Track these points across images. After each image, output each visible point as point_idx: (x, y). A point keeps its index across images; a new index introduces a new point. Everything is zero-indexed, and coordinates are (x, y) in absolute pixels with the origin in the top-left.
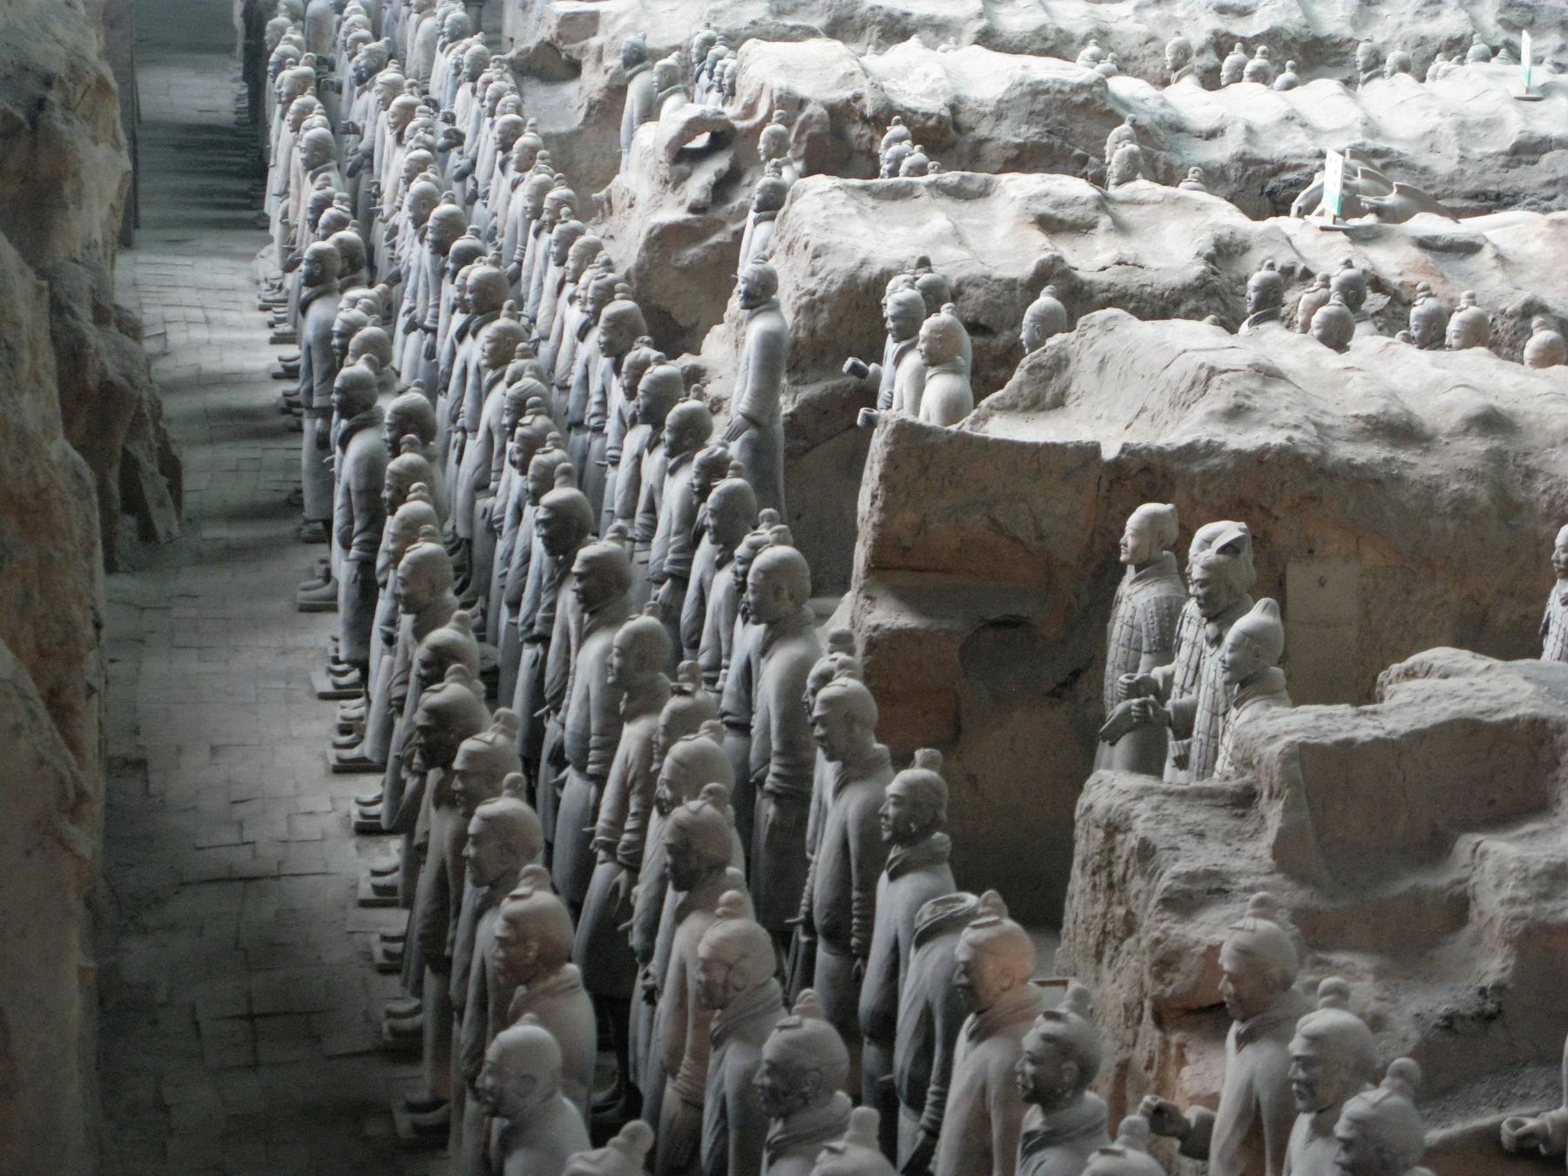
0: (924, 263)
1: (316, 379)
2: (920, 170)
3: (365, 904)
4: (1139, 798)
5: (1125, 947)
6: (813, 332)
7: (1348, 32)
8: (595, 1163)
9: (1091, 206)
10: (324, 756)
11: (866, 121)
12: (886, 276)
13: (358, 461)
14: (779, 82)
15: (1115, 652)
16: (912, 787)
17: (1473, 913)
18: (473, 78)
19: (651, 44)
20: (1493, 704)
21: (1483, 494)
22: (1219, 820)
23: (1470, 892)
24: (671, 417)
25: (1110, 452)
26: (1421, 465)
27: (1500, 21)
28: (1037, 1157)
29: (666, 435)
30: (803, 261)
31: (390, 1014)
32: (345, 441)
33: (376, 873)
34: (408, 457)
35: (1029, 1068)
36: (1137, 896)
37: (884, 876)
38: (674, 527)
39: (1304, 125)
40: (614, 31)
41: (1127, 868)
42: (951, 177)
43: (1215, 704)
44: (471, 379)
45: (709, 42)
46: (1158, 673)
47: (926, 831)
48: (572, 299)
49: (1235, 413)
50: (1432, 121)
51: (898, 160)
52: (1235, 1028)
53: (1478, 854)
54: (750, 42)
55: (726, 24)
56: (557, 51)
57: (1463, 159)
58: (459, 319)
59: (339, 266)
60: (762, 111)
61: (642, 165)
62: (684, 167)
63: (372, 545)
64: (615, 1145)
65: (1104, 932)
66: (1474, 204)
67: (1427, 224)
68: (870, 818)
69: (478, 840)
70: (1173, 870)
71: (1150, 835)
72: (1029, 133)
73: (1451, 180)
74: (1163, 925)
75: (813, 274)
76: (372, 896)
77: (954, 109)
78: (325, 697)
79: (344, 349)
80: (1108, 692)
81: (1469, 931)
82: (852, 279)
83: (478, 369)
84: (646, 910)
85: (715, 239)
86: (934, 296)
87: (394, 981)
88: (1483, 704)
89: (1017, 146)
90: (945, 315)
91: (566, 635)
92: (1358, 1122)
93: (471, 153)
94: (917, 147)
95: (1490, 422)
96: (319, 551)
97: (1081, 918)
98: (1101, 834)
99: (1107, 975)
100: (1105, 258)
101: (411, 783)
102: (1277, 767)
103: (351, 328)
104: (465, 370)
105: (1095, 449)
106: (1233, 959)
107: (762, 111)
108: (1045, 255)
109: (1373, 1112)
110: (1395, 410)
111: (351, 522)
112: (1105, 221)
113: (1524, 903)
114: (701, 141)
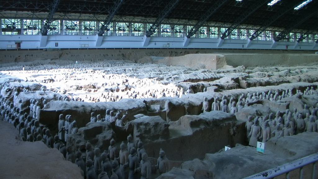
2: (28, 91)
14: (14, 85)
15: (59, 126)
17: (99, 140)
21: (83, 111)
22: (79, 136)
25: (56, 111)
26: (78, 110)
37: (54, 143)
45: (5, 83)
46: (64, 127)
49: (65, 107)
52: (87, 151)
55: (6, 81)
70: (76, 141)
72: (34, 88)
77: (28, 86)
82: (27, 100)
86: (35, 101)
92: (103, 155)
95: (83, 106)
98: (70, 139)
105: (55, 111)
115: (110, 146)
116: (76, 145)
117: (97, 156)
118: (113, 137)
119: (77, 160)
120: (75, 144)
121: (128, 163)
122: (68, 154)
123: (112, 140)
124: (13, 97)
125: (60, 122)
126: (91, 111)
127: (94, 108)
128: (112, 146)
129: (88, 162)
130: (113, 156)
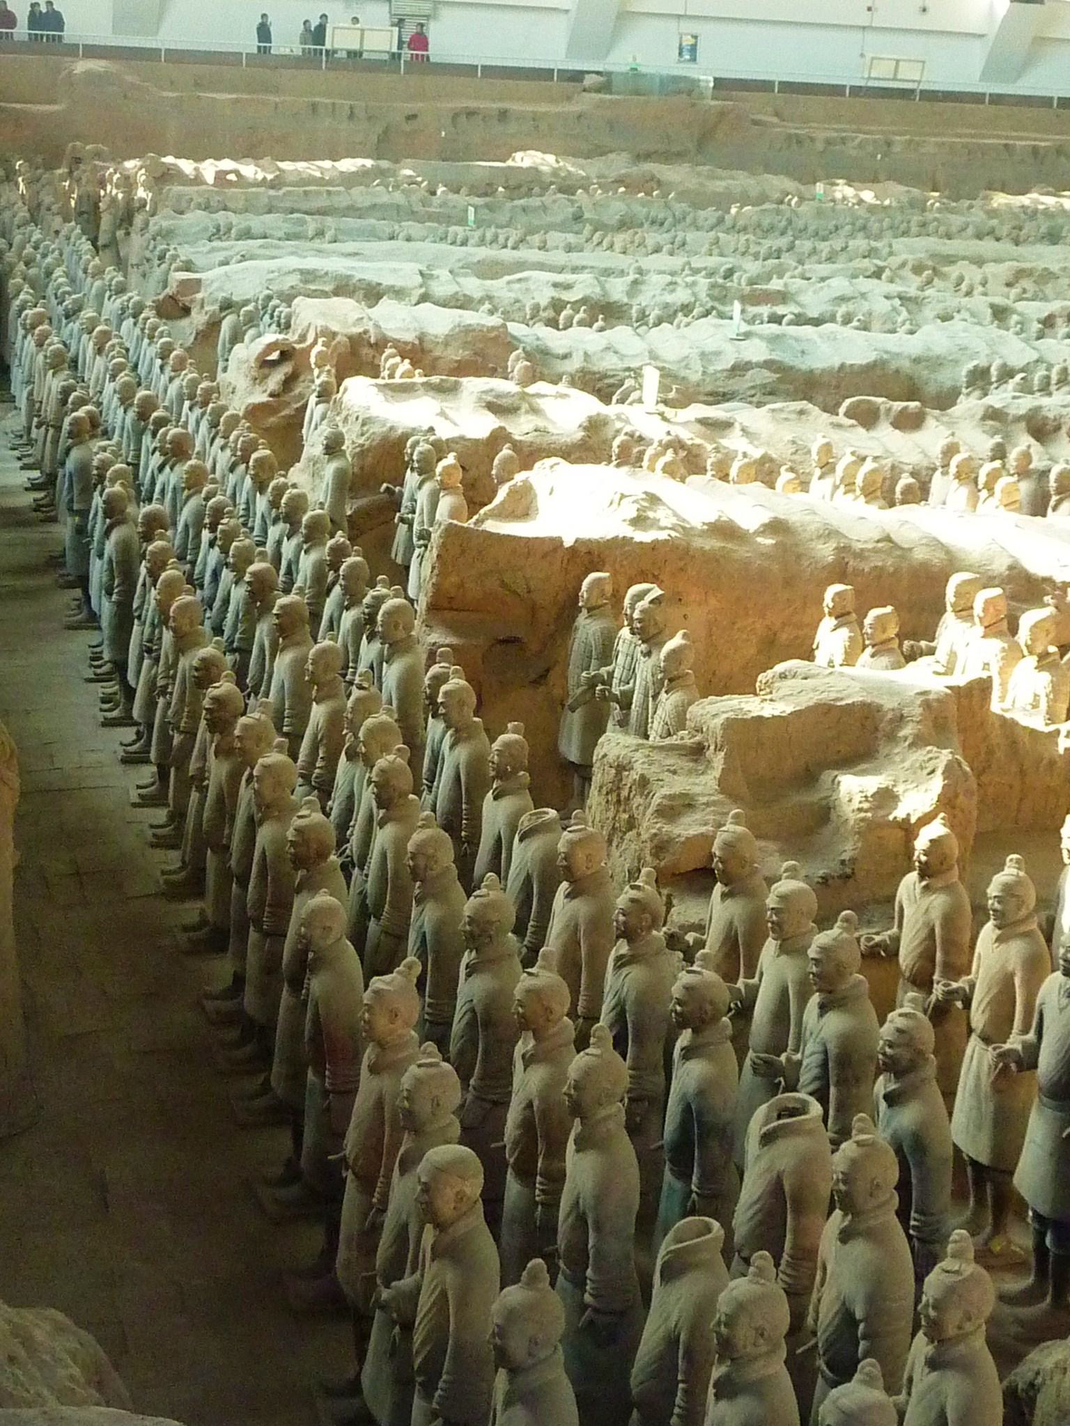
0: (431, 430)
1: (75, 492)
3: (135, 805)
4: (637, 750)
5: (627, 836)
6: (362, 468)
7: (626, 300)
8: (388, 984)
9: (517, 397)
10: (94, 717)
11: (371, 346)
12: (405, 437)
13: (117, 544)
14: (320, 323)
16: (507, 745)
17: (833, 816)
18: (135, 316)
19: (235, 298)
20: (839, 695)
22: (686, 764)
23: (831, 805)
24: (305, 519)
25: (568, 543)
26: (742, 552)
27: (708, 295)
28: (625, 971)
29: (303, 530)
30: (357, 428)
31: (163, 873)
32: (107, 533)
33: (139, 787)
34: (158, 543)
35: (621, 918)
36: (637, 808)
37: (490, 795)
38: (308, 584)
39: (616, 352)
40: (210, 290)
41: (630, 792)
42: (435, 379)
43: (646, 689)
44: (169, 496)
45: (269, 298)
47: (515, 771)
48: (223, 448)
50: (686, 352)
51: (395, 367)
52: (719, 888)
53: (835, 784)
54: (299, 298)
55: (275, 287)
56: (176, 301)
57: (704, 373)
58: (157, 459)
59: (88, 427)
60: (310, 340)
61: (239, 369)
62: (266, 371)
63: (128, 593)
64: (398, 972)
65: (613, 828)
66: (711, 399)
67: (699, 410)
68: (476, 764)
69: (260, 779)
71: (645, 772)
73: (698, 385)
74: (658, 825)
75: (362, 435)
76: (138, 800)
77: (421, 338)
78: (90, 681)
79: (101, 478)
80: (571, 682)
81: (830, 827)
83: (174, 488)
84: (340, 815)
85: (286, 412)
87: (159, 854)
88: (833, 695)
89: (458, 362)
90: (450, 459)
91: (262, 649)
92: (824, 949)
93: (134, 359)
94: (407, 361)
96: (78, 592)
97: (598, 819)
98: (613, 771)
99: (615, 853)
100: (530, 427)
101: (177, 739)
102: (719, 733)
103: (104, 466)
104: (163, 491)
106: (721, 849)
107: (310, 340)
108: (496, 426)
109: (831, 943)
110: (724, 519)
111: (112, 579)
112: (525, 406)
113: (866, 811)
114: (275, 356)
115: (913, 876)
116: (649, 826)
117: (783, 950)
118: (947, 802)
119: (619, 958)
120: (645, 825)
121: (1031, 1036)
122: (570, 896)
123: (936, 829)
124: (305, 407)
125: (587, 628)
126: (839, 572)
127: (860, 555)
128: (922, 876)
129: (688, 988)
130: (927, 956)
